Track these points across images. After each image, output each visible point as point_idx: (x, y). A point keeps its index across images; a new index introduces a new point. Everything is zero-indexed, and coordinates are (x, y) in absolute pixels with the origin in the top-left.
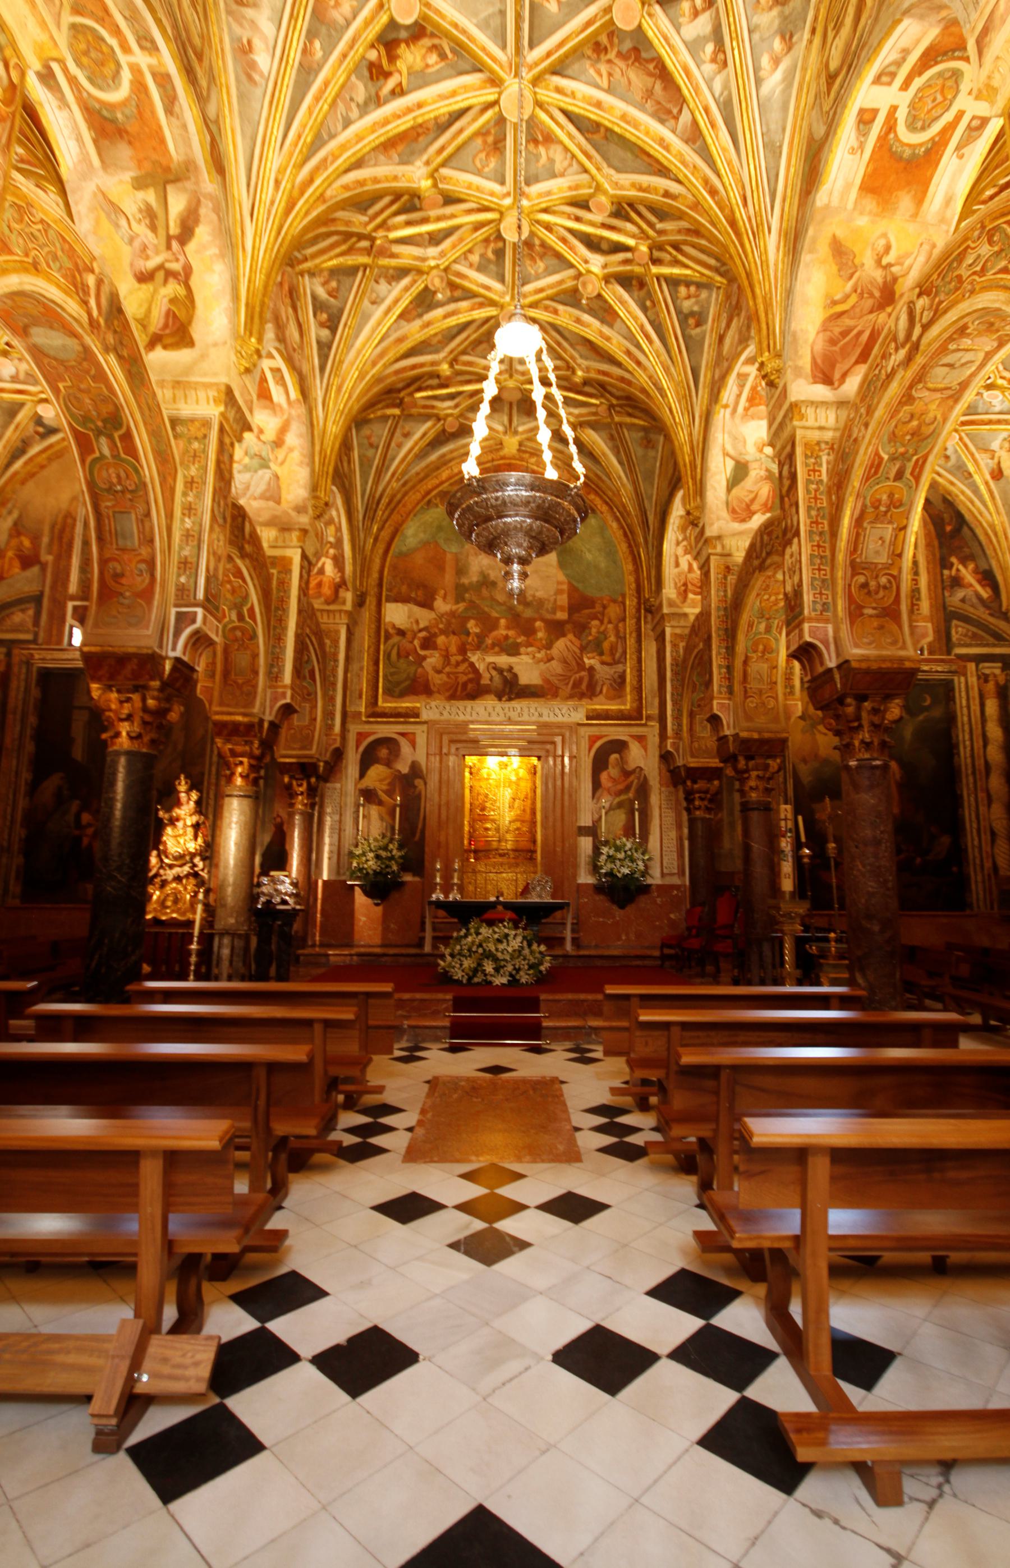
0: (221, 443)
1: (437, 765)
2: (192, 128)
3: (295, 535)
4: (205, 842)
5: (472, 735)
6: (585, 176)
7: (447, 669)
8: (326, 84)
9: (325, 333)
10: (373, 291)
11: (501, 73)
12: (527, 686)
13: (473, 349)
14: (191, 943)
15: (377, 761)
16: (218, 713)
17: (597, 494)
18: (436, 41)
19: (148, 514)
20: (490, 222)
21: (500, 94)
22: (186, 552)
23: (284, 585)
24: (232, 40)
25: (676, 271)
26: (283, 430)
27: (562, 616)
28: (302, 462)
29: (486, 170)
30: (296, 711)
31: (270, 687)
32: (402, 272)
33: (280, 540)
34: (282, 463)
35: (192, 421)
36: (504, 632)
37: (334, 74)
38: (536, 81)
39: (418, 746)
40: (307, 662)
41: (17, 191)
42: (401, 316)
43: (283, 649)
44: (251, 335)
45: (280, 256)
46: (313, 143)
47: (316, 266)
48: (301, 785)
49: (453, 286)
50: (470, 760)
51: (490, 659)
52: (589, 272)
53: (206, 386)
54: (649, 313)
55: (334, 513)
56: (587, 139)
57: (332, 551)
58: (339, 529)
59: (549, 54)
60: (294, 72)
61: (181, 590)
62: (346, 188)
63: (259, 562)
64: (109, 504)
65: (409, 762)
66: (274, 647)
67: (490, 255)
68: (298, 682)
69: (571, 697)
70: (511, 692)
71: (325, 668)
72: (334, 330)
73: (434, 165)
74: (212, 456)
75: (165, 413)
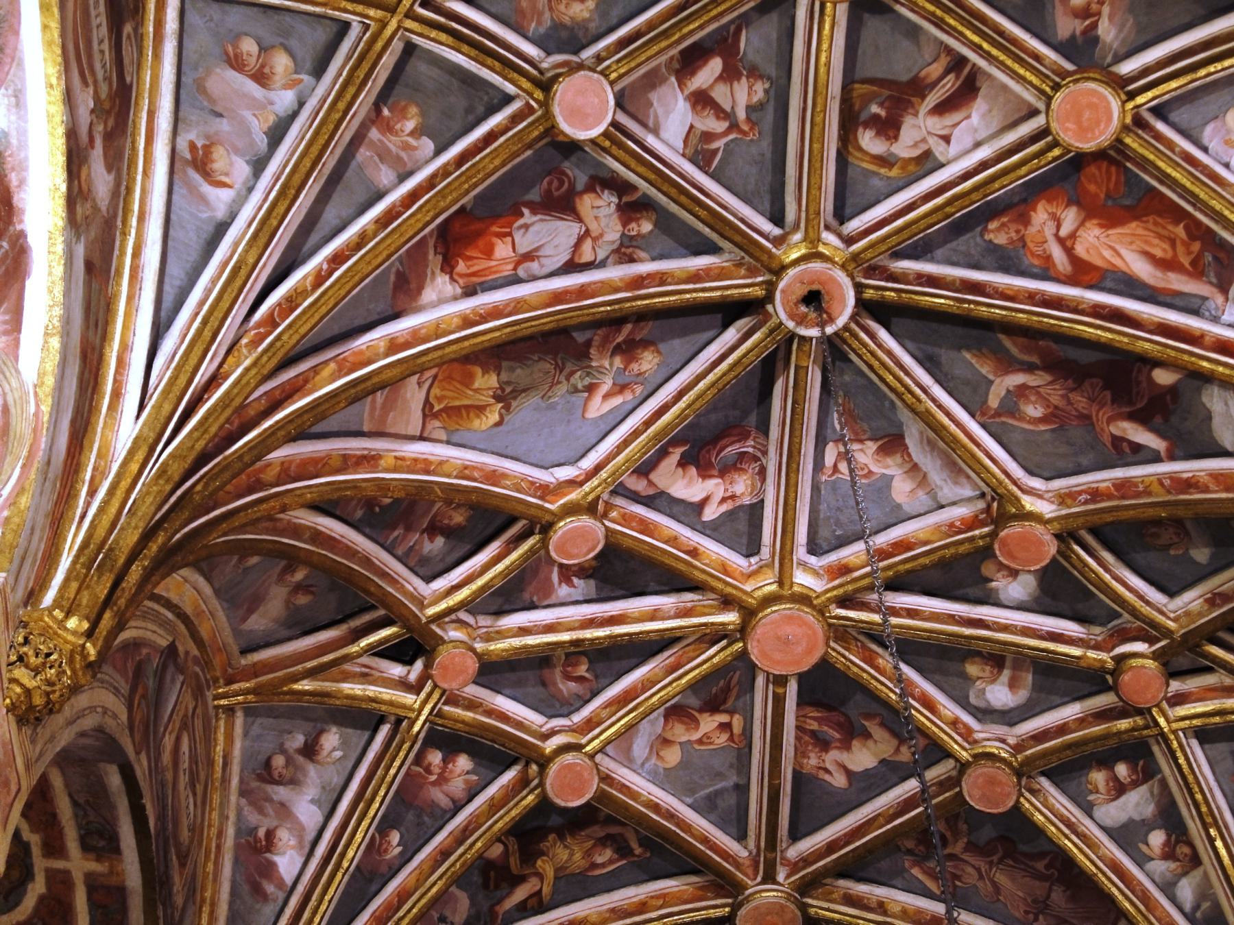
18: (614, 830)
21: (735, 908)
59: (832, 847)
60: (347, 878)
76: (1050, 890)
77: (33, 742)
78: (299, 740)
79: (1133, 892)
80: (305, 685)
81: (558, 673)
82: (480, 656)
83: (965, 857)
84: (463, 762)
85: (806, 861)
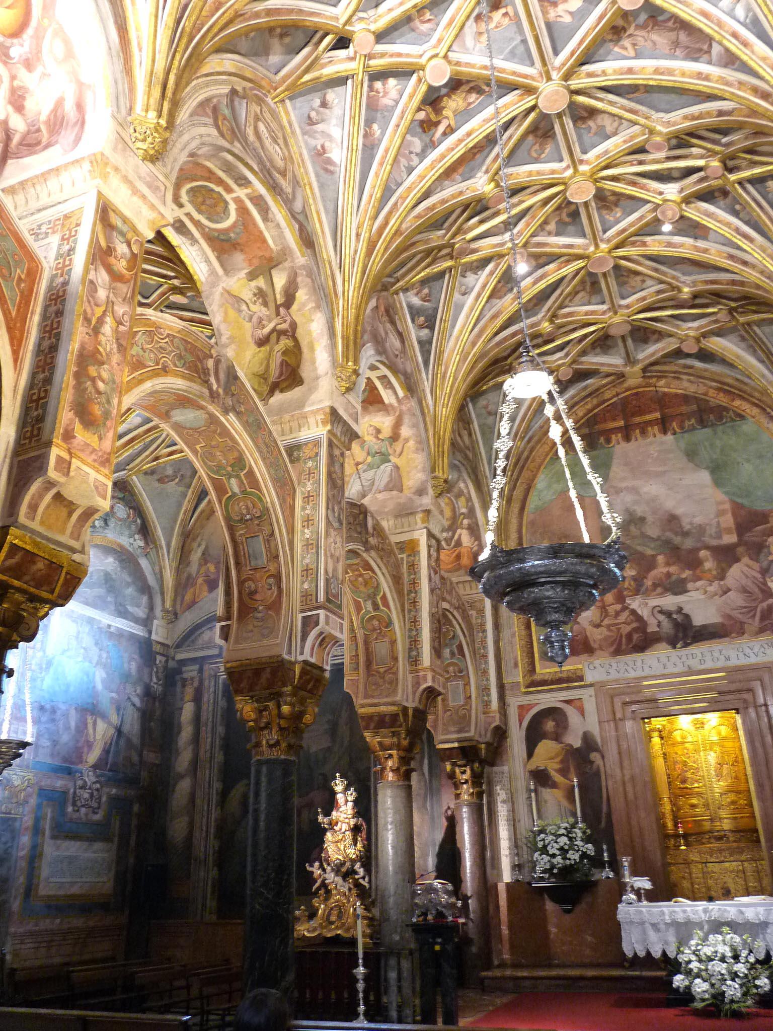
0: (331, 456)
1: (613, 733)
2: (283, 224)
3: (419, 517)
4: (364, 847)
5: (647, 693)
6: (637, 127)
7: (606, 622)
8: (387, 151)
9: (426, 332)
10: (461, 285)
11: (535, 84)
12: (704, 627)
13: (571, 301)
14: (357, 966)
15: (544, 736)
16: (363, 706)
17: (742, 398)
19: (272, 534)
20: (556, 194)
21: (537, 98)
22: (307, 561)
23: (413, 567)
24: (309, 150)
25: (757, 171)
26: (397, 425)
27: (730, 539)
28: (417, 449)
29: (543, 156)
30: (440, 694)
31: (411, 672)
32: (485, 262)
33: (406, 525)
34: (400, 455)
35: (306, 444)
36: (665, 570)
37: (391, 141)
38: (567, 77)
39: (586, 714)
40: (454, 637)
41: (147, 322)
42: (491, 297)
43: (418, 631)
44: (348, 361)
45: (367, 290)
46: (382, 196)
47: (407, 283)
48: (464, 772)
49: (536, 256)
50: (657, 723)
51: (654, 602)
52: (666, 201)
53: (315, 412)
54: (741, 216)
55: (462, 485)
56: (629, 99)
57: (466, 522)
58: (469, 499)
59: (572, 54)
61: (305, 595)
62: (418, 217)
63: (385, 551)
64: (242, 532)
65: (580, 734)
66: (410, 630)
67: (567, 219)
68: (438, 662)
69: (761, 631)
70: (685, 637)
71: (473, 641)
72: (432, 328)
73: (492, 171)
74: (323, 469)
75: (279, 443)
76: (678, 35)
77: (165, 166)
78: (317, 102)
79: (712, 22)
80: (307, 77)
81: (417, 23)
82: (374, 33)
83: (635, 33)
84: (392, 82)
85: (564, 65)
